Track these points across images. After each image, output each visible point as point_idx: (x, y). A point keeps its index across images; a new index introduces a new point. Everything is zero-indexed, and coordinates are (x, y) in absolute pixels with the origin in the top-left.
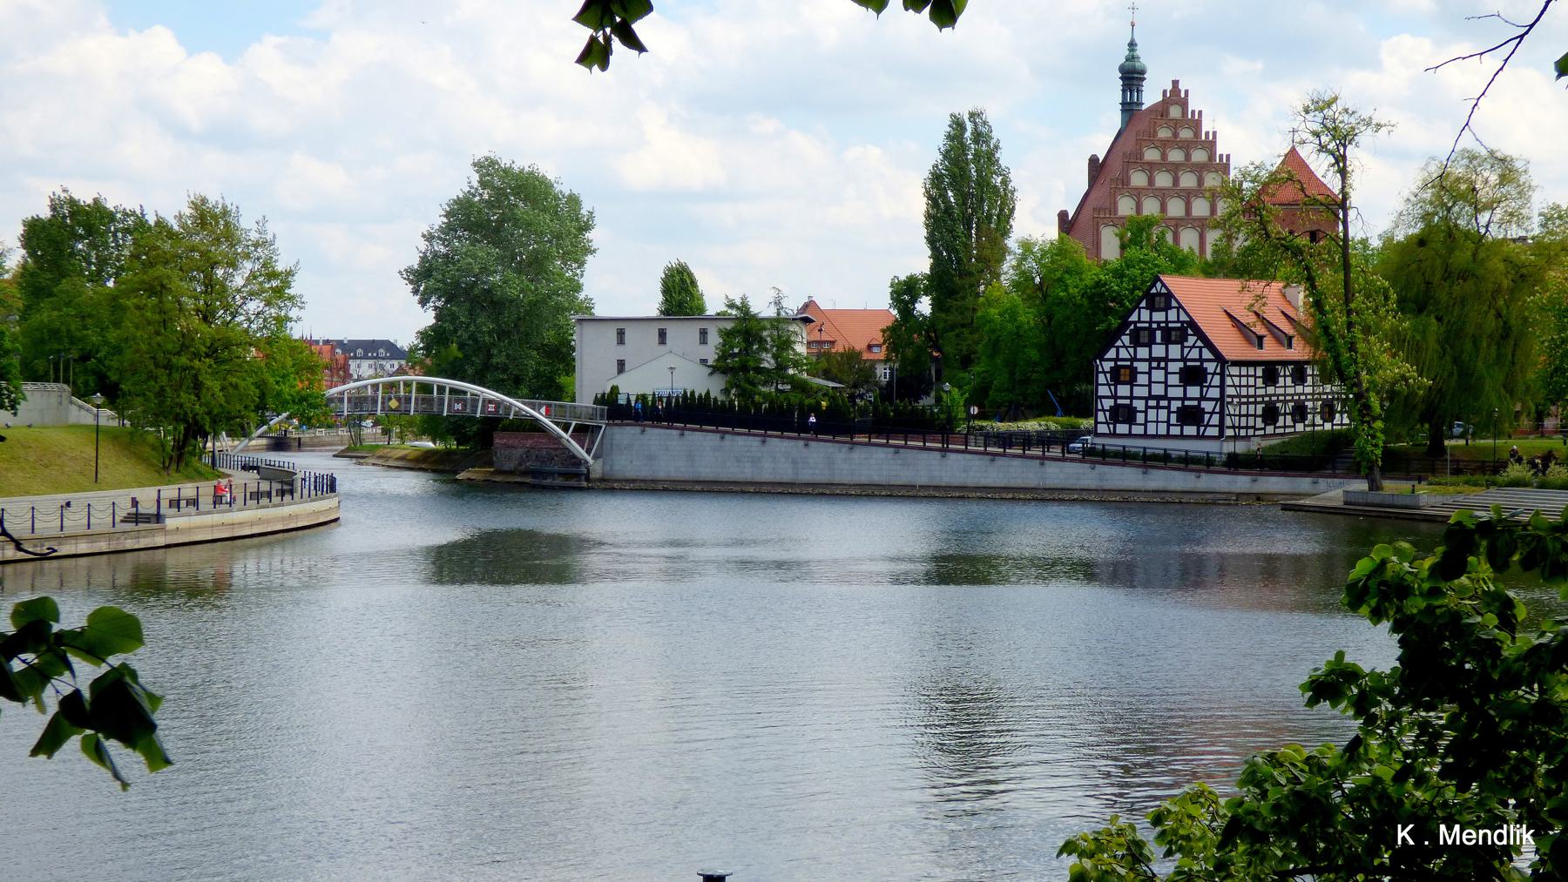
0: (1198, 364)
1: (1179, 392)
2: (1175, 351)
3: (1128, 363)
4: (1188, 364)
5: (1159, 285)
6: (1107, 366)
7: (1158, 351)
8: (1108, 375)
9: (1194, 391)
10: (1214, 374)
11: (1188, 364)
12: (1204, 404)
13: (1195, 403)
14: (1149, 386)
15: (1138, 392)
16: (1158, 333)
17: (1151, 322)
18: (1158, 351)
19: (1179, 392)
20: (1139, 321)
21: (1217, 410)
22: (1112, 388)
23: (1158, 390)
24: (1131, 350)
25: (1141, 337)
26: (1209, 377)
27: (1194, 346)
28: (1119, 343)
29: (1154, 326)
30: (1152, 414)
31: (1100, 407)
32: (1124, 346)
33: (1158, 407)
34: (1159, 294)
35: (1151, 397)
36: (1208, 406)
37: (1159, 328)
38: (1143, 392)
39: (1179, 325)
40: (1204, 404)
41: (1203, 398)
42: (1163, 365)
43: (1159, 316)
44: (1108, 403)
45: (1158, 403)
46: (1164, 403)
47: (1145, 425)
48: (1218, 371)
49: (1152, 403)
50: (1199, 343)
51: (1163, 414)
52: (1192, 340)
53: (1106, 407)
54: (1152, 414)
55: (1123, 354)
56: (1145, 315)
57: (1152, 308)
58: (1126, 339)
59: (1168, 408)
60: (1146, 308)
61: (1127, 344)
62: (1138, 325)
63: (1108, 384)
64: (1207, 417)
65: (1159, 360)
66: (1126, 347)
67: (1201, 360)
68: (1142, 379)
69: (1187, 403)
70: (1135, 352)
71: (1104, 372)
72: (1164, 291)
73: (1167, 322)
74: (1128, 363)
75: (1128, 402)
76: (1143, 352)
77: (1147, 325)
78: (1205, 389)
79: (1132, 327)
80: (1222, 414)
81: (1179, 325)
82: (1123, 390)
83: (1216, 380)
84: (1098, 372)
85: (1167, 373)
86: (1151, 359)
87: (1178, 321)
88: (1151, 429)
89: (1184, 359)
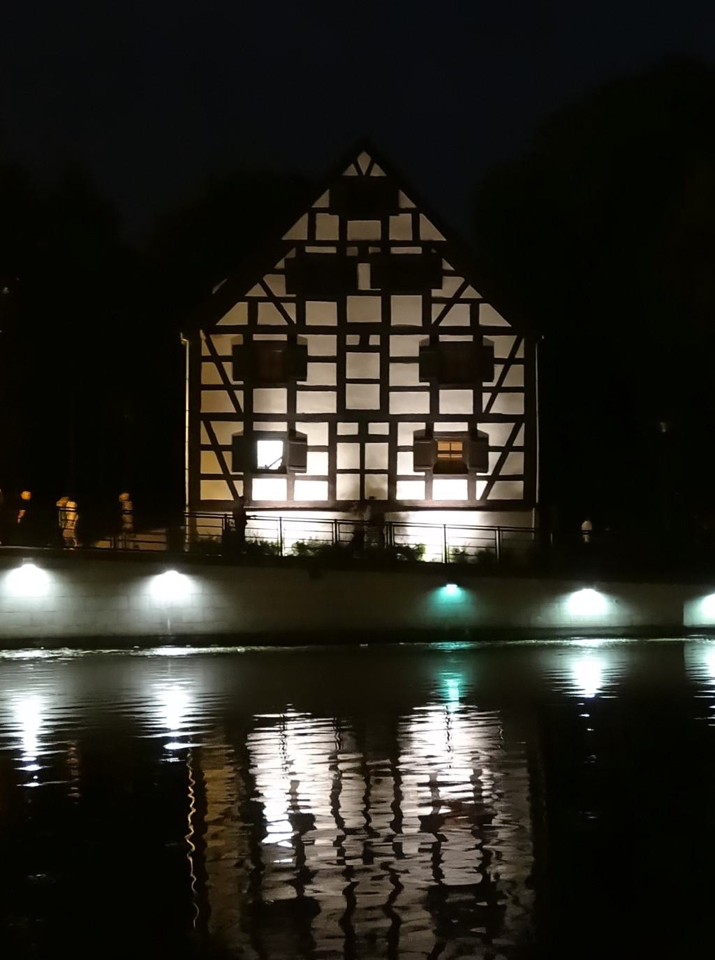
0: (469, 338)
1: (419, 403)
2: (407, 309)
3: (284, 337)
4: (444, 338)
5: (364, 160)
6: (225, 345)
7: (365, 309)
8: (228, 367)
9: (457, 401)
10: (508, 362)
11: (444, 338)
12: (481, 427)
13: (463, 427)
15: (308, 403)
16: (364, 271)
17: (342, 243)
18: (365, 309)
19: (419, 403)
20: (312, 240)
21: (519, 441)
22: (240, 395)
23: (364, 398)
24: (291, 309)
27: (456, 299)
28: (257, 291)
29: (353, 251)
30: (347, 456)
31: (205, 440)
32: (271, 298)
33: (363, 438)
34: (364, 179)
36: (495, 434)
37: (363, 257)
38: (326, 403)
39: (418, 250)
40: (481, 427)
41: (480, 415)
42: (375, 340)
43: (365, 229)
45: (363, 429)
46: (380, 428)
47: (331, 479)
48: (520, 354)
50: (470, 293)
51: (378, 454)
52: (450, 286)
53: (225, 438)
55: (268, 314)
56: (328, 226)
59: (391, 438)
60: (328, 211)
62: (309, 249)
63: (227, 386)
64: (493, 458)
65: (364, 330)
66: (278, 302)
67: (475, 328)
68: (320, 374)
69: (439, 427)
70: (301, 313)
71: (217, 360)
72: (377, 172)
73: (385, 243)
74: (284, 337)
76: (321, 312)
77: (332, 250)
78: (486, 397)
79: (292, 254)
80: (528, 449)
81: (418, 250)
83: (516, 377)
84: (197, 360)
85: (386, 361)
86: (343, 328)
88: (346, 487)
89: (430, 328)
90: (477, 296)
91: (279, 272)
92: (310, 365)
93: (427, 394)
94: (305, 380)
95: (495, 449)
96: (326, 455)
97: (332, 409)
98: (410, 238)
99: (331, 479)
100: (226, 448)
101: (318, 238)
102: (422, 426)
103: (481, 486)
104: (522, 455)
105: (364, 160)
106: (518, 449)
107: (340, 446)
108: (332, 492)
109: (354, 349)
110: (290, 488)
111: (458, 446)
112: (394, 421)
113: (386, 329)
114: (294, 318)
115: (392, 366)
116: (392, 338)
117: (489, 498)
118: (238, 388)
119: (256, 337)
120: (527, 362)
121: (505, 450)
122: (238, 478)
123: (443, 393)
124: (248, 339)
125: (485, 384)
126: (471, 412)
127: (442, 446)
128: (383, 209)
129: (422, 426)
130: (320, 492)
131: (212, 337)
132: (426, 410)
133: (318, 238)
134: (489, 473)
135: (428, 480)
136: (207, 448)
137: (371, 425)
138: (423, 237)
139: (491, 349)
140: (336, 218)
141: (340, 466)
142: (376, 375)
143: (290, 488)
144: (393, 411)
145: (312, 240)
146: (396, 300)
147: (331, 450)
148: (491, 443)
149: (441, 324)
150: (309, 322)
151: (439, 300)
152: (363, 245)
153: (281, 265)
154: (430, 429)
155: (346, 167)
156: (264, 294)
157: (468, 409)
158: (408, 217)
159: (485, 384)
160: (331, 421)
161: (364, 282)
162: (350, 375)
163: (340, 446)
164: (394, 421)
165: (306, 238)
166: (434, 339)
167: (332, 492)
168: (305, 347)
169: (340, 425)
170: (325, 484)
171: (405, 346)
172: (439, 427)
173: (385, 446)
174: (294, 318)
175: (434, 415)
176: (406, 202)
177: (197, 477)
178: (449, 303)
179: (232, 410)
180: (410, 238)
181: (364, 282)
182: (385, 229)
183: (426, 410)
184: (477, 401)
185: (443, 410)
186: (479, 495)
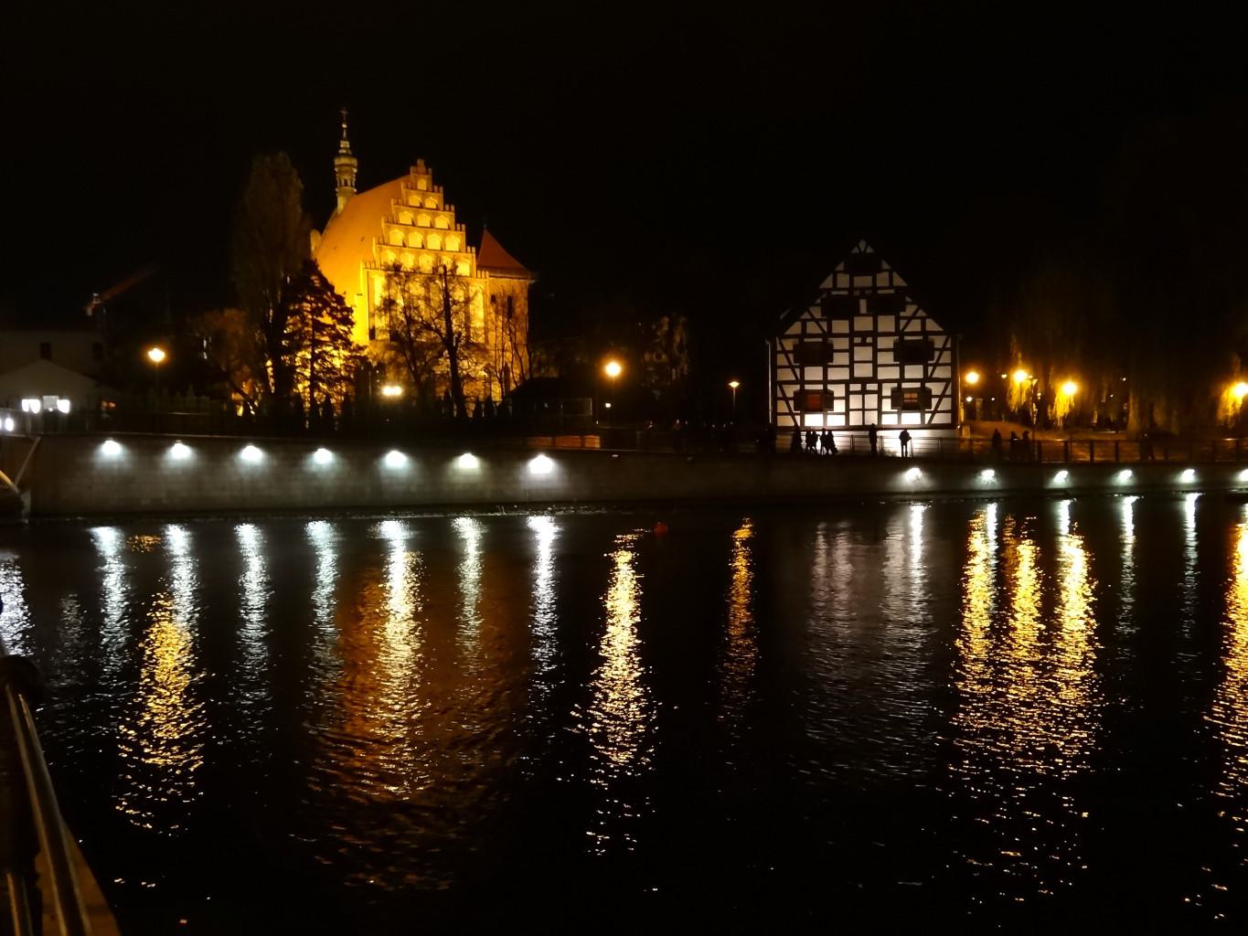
0: (920, 338)
1: (894, 373)
2: (886, 323)
3: (820, 340)
5: (862, 245)
6: (789, 345)
7: (863, 324)
8: (791, 356)
9: (914, 371)
12: (928, 385)
13: (918, 385)
14: (851, 367)
16: (863, 304)
17: (851, 288)
19: (894, 373)
21: (949, 392)
22: (798, 371)
23: (863, 371)
24: (824, 325)
25: (843, 308)
26: (937, 354)
27: (914, 317)
28: (806, 316)
29: (857, 293)
30: (855, 402)
31: (780, 395)
33: (864, 392)
35: (853, 380)
36: (936, 389)
37: (863, 296)
38: (845, 375)
39: (892, 291)
40: (928, 385)
41: (927, 378)
42: (869, 340)
43: (863, 281)
44: (791, 391)
45: (864, 387)
46: (871, 387)
47: (847, 414)
48: (949, 345)
49: (855, 387)
50: (921, 313)
51: (872, 401)
52: (910, 310)
54: (855, 402)
55: (812, 328)
56: (843, 280)
57: (853, 271)
58: (817, 312)
59: (879, 392)
60: (844, 272)
61: (818, 315)
62: (834, 293)
64: (934, 401)
65: (864, 335)
66: (817, 321)
67: (924, 332)
68: (841, 358)
69: (905, 385)
71: (785, 352)
72: (870, 250)
73: (874, 288)
74: (820, 340)
75: (820, 387)
76: (841, 326)
77: (845, 293)
78: (930, 369)
79: (824, 295)
81: (892, 291)
82: (813, 373)
83: (946, 357)
84: (775, 353)
85: (876, 351)
86: (852, 334)
87: (891, 286)
88: (855, 419)
89: (899, 332)
90: (924, 314)
91: (818, 305)
92: (835, 355)
93: (898, 368)
94: (832, 362)
95: (936, 396)
96: (844, 401)
97: (847, 377)
98: (888, 285)
99: (847, 414)
100: (791, 399)
101: (839, 286)
102: (895, 385)
103: (928, 416)
104: (950, 399)
105: (862, 245)
106: (948, 396)
107: (851, 396)
108: (847, 420)
109: (858, 345)
110: (825, 419)
111: (915, 395)
112: (880, 383)
113: (875, 334)
114: (826, 329)
115: (879, 354)
116: (880, 340)
117: (933, 422)
118: (796, 367)
119: (806, 340)
120: (952, 350)
121: (941, 397)
122: (797, 414)
123: (906, 367)
124: (801, 340)
125: (930, 362)
126: (921, 377)
127: (907, 396)
128: (873, 270)
129: (895, 385)
130: (841, 421)
131: (784, 342)
132: (897, 376)
133: (839, 286)
134: (932, 409)
135: (899, 414)
136: (781, 399)
137: (868, 385)
138: (895, 284)
139: (932, 343)
140: (847, 277)
141: (851, 407)
142: (871, 359)
143: (825, 419)
144: (880, 377)
145: (835, 287)
146: (881, 319)
147: (847, 399)
148: (933, 393)
149: (906, 330)
150: (834, 331)
151: (904, 318)
152: (862, 290)
153: (819, 301)
154: (900, 386)
155: (852, 248)
156: (809, 317)
157: (921, 377)
158: (886, 275)
159: (930, 362)
160: (847, 383)
161: (863, 309)
162: (856, 359)
163: (851, 396)
164: (880, 383)
165: (831, 286)
166: (901, 339)
167: (847, 420)
168: (832, 345)
169: (851, 385)
170: (844, 416)
171: (885, 342)
172: (905, 385)
173: (876, 395)
174: (826, 329)
175: (902, 379)
176: (885, 266)
177: (776, 414)
178: (909, 319)
179: (794, 378)
180: (888, 285)
181: (863, 309)
182: (874, 280)
183: (897, 376)
184: (925, 371)
185: (907, 376)
186: (926, 422)
